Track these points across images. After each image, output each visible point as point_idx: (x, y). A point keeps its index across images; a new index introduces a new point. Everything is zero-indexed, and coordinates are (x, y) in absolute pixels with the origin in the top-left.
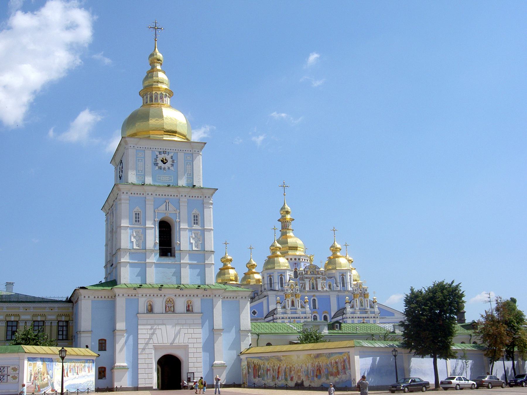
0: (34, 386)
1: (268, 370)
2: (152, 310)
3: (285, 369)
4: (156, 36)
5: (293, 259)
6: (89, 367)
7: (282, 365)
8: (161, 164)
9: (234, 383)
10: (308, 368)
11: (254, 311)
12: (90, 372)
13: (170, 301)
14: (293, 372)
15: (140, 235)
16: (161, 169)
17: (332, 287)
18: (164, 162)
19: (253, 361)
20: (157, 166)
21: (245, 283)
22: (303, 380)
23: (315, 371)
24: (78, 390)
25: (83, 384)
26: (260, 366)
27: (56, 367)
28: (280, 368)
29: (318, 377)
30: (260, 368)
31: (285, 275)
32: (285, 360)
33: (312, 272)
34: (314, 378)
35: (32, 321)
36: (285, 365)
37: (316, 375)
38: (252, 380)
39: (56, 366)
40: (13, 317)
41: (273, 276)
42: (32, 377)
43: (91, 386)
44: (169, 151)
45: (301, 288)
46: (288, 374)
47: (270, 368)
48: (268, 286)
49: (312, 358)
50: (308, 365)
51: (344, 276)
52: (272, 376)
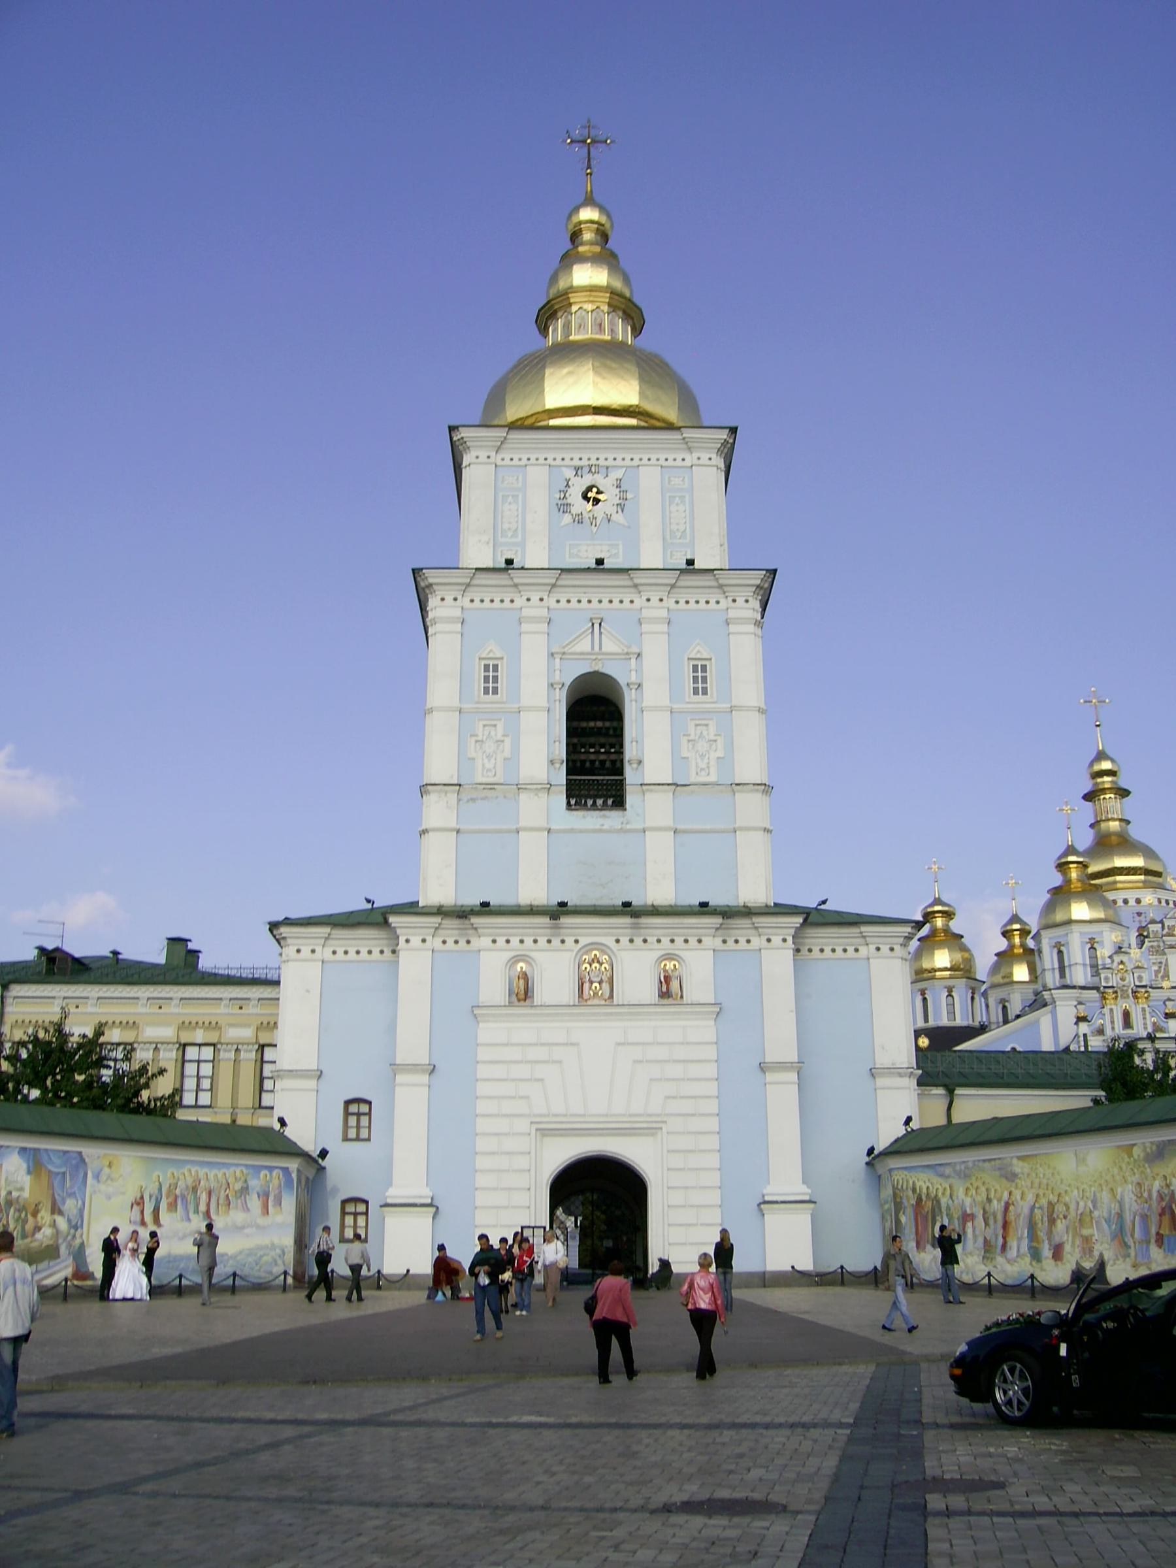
1: (966, 1217)
2: (529, 994)
3: (1032, 1208)
5: (1130, 900)
6: (267, 1195)
7: (1019, 1197)
8: (579, 506)
9: (842, 1267)
10: (1121, 1204)
13: (598, 962)
14: (1060, 1225)
15: (499, 737)
16: (581, 522)
19: (914, 1182)
20: (567, 514)
21: (998, 979)
22: (1101, 1255)
23: (1154, 1219)
24: (181, 1276)
25: (234, 1257)
26: (938, 1202)
27: (102, 1187)
28: (1011, 1208)
29: (1165, 1241)
30: (936, 1210)
31: (1103, 941)
32: (1028, 1175)
34: (1148, 1249)
35: (177, 1046)
36: (1031, 1195)
37: (1158, 1234)
39: (99, 1181)
40: (119, 1030)
41: (1068, 943)
43: (276, 1264)
44: (610, 462)
45: (1156, 976)
46: (1042, 1234)
47: (975, 1210)
48: (1053, 973)
49: (1135, 1161)
50: (1122, 1193)
52: (981, 1240)
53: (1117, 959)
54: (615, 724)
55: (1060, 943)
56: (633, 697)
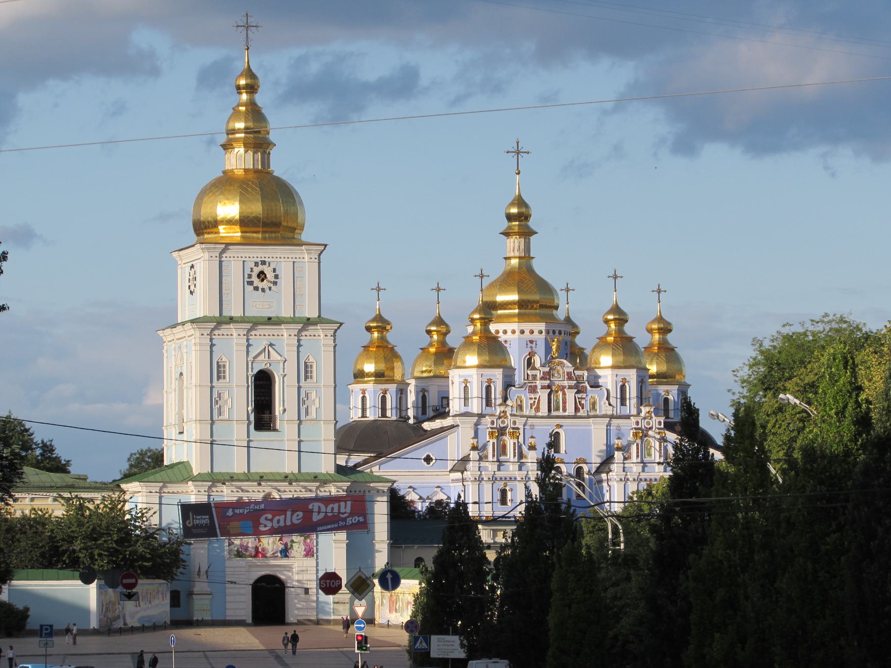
0: (105, 619)
4: (247, 40)
8: (257, 282)
11: (428, 456)
12: (164, 598)
17: (597, 407)
18: (262, 276)
24: (154, 624)
30: (398, 599)
33: (556, 375)
38: (387, 615)
42: (104, 608)
44: (270, 260)
45: (531, 408)
51: (626, 384)
53: (502, 408)
54: (268, 383)
55: (467, 380)
56: (281, 381)
